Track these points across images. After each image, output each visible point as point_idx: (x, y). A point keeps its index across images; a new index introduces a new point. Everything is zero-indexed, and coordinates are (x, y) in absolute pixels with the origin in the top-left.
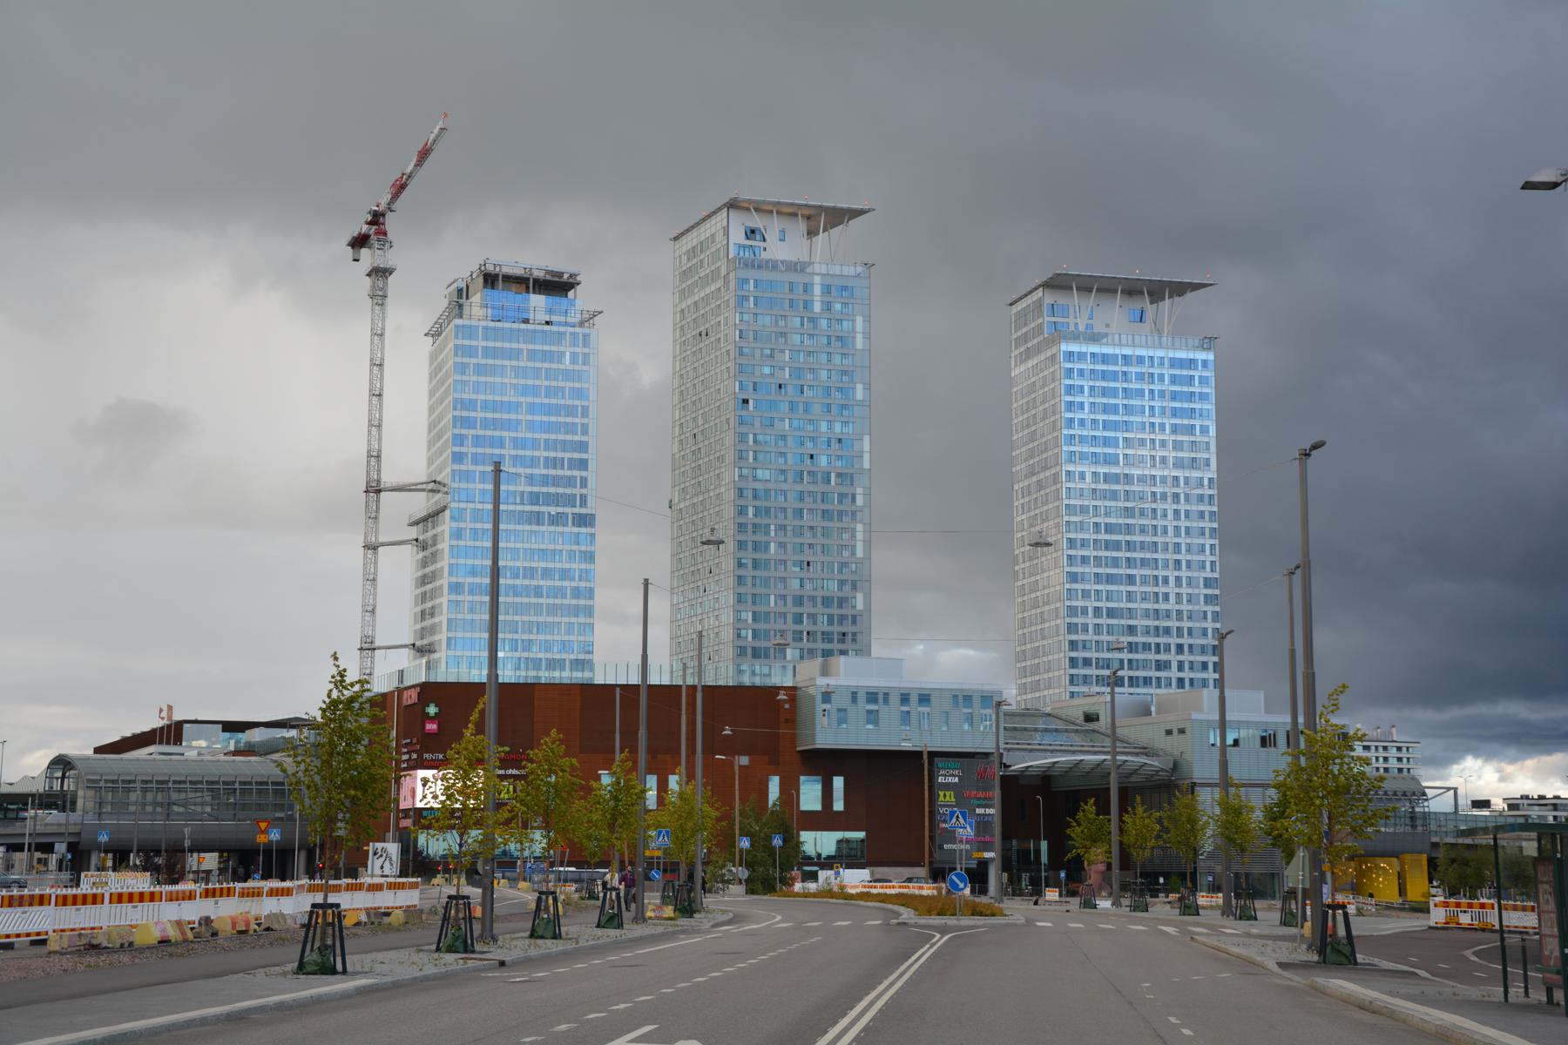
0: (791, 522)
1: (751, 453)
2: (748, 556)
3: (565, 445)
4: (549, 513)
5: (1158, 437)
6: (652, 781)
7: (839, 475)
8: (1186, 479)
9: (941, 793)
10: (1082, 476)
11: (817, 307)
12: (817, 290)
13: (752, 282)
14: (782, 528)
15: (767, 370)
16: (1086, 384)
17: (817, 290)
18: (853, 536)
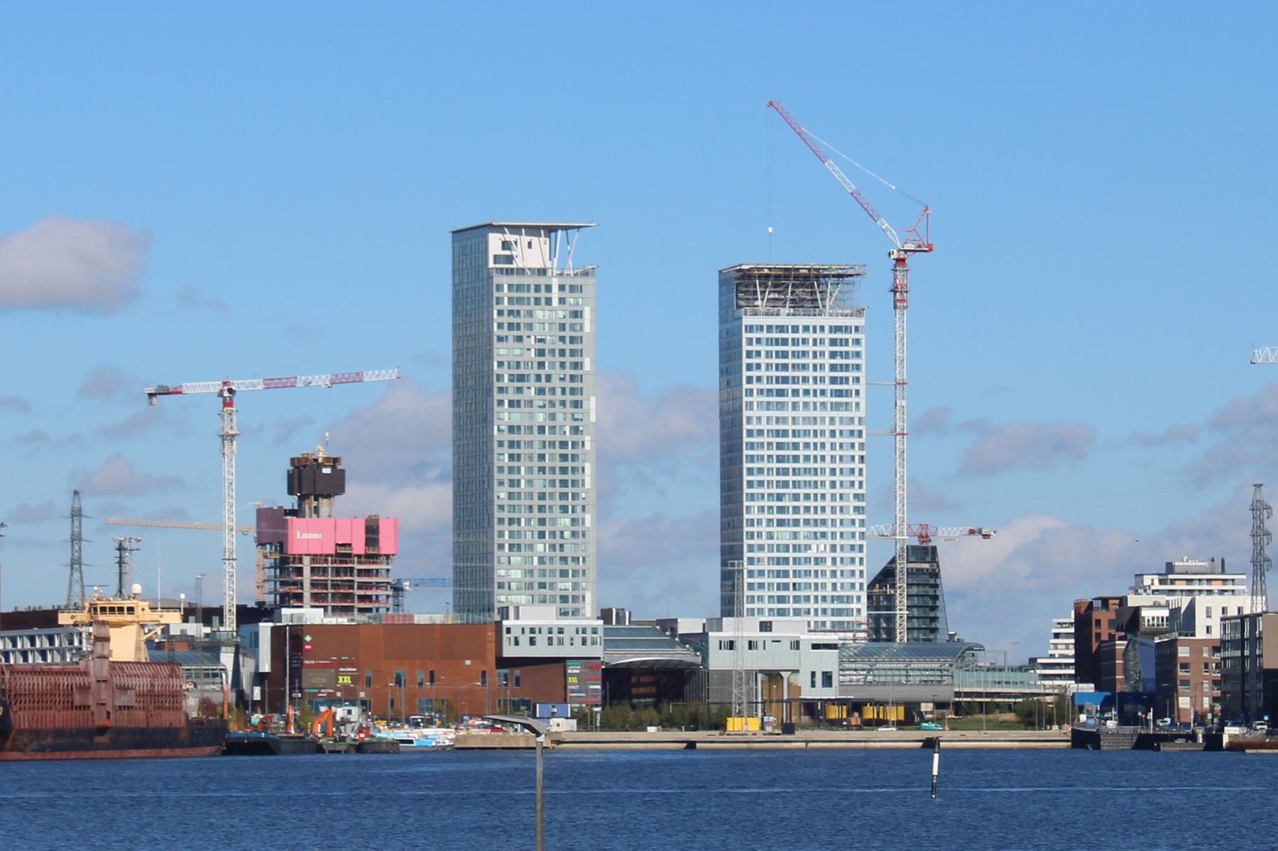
8: (841, 419)
12: (555, 289)
15: (518, 352)
17: (555, 289)
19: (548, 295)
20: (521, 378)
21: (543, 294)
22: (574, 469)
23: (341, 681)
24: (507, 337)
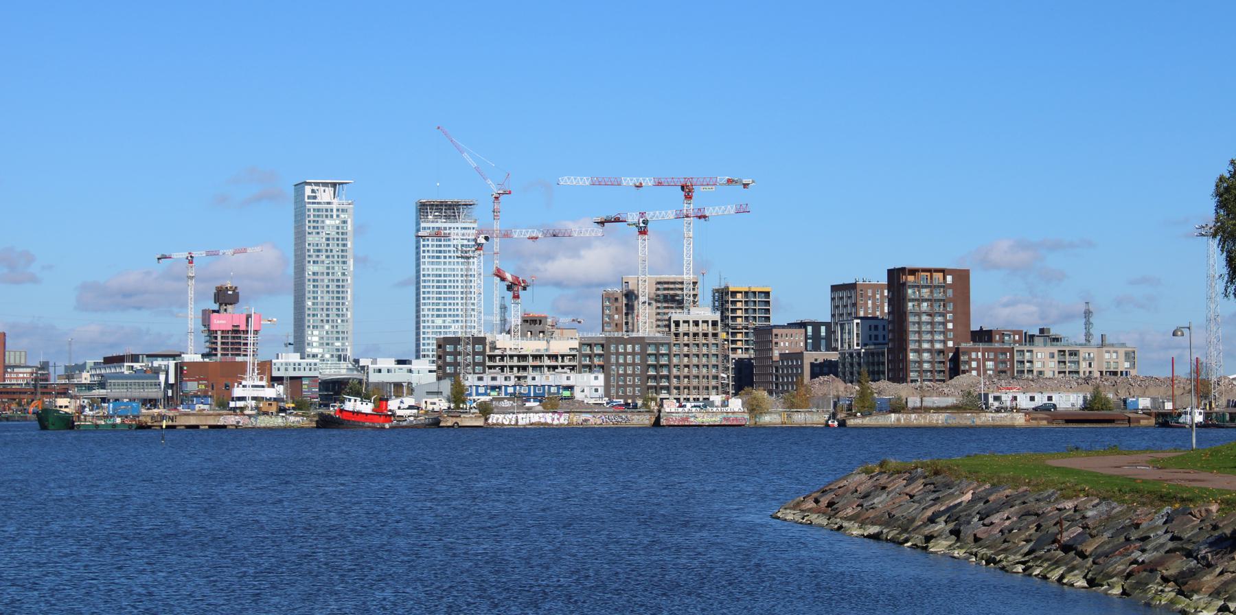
15: (317, 239)
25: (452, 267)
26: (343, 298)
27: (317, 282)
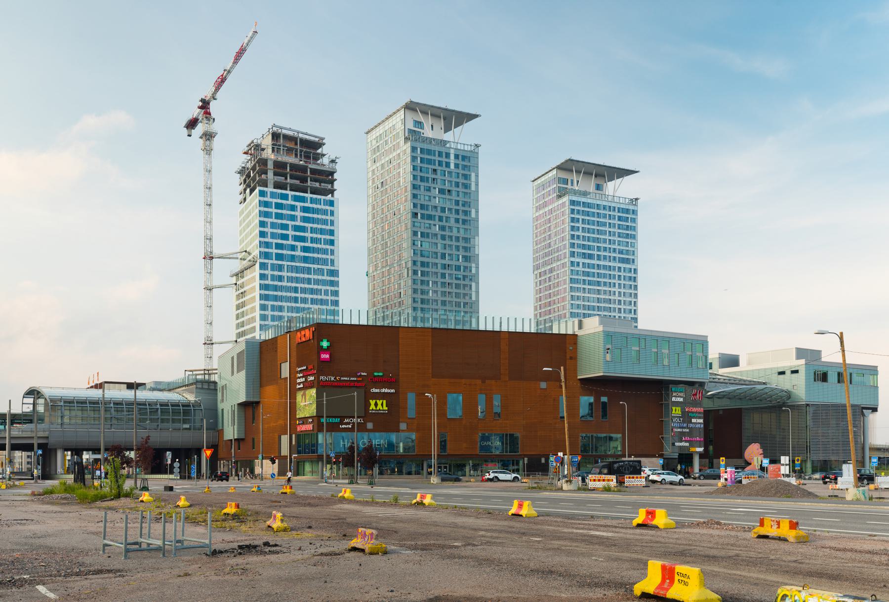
0: (440, 280)
1: (419, 242)
2: (419, 296)
3: (322, 232)
4: (314, 268)
5: (613, 247)
6: (482, 398)
7: (463, 257)
9: (674, 408)
10: (578, 264)
11: (452, 166)
12: (452, 157)
13: (419, 149)
14: (436, 283)
16: (581, 217)
17: (452, 157)
18: (471, 288)
19: (447, 160)
20: (430, 217)
21: (444, 159)
22: (465, 286)
23: (372, 407)
24: (420, 186)
25: (607, 263)
26: (465, 295)
27: (428, 267)
